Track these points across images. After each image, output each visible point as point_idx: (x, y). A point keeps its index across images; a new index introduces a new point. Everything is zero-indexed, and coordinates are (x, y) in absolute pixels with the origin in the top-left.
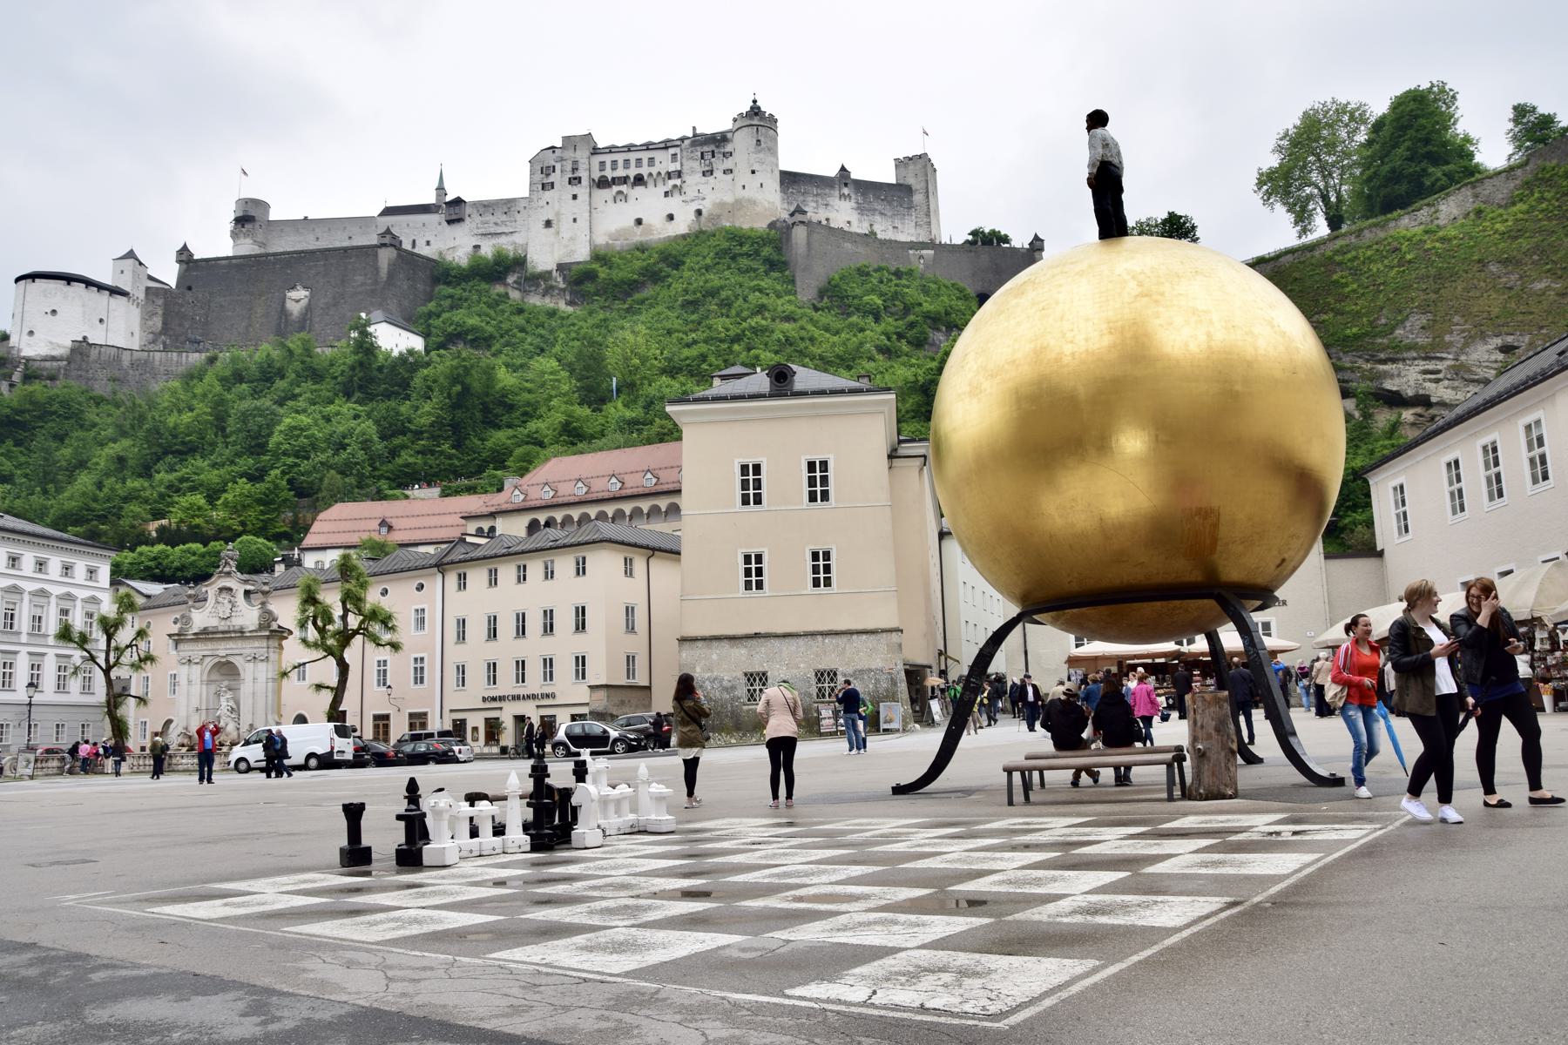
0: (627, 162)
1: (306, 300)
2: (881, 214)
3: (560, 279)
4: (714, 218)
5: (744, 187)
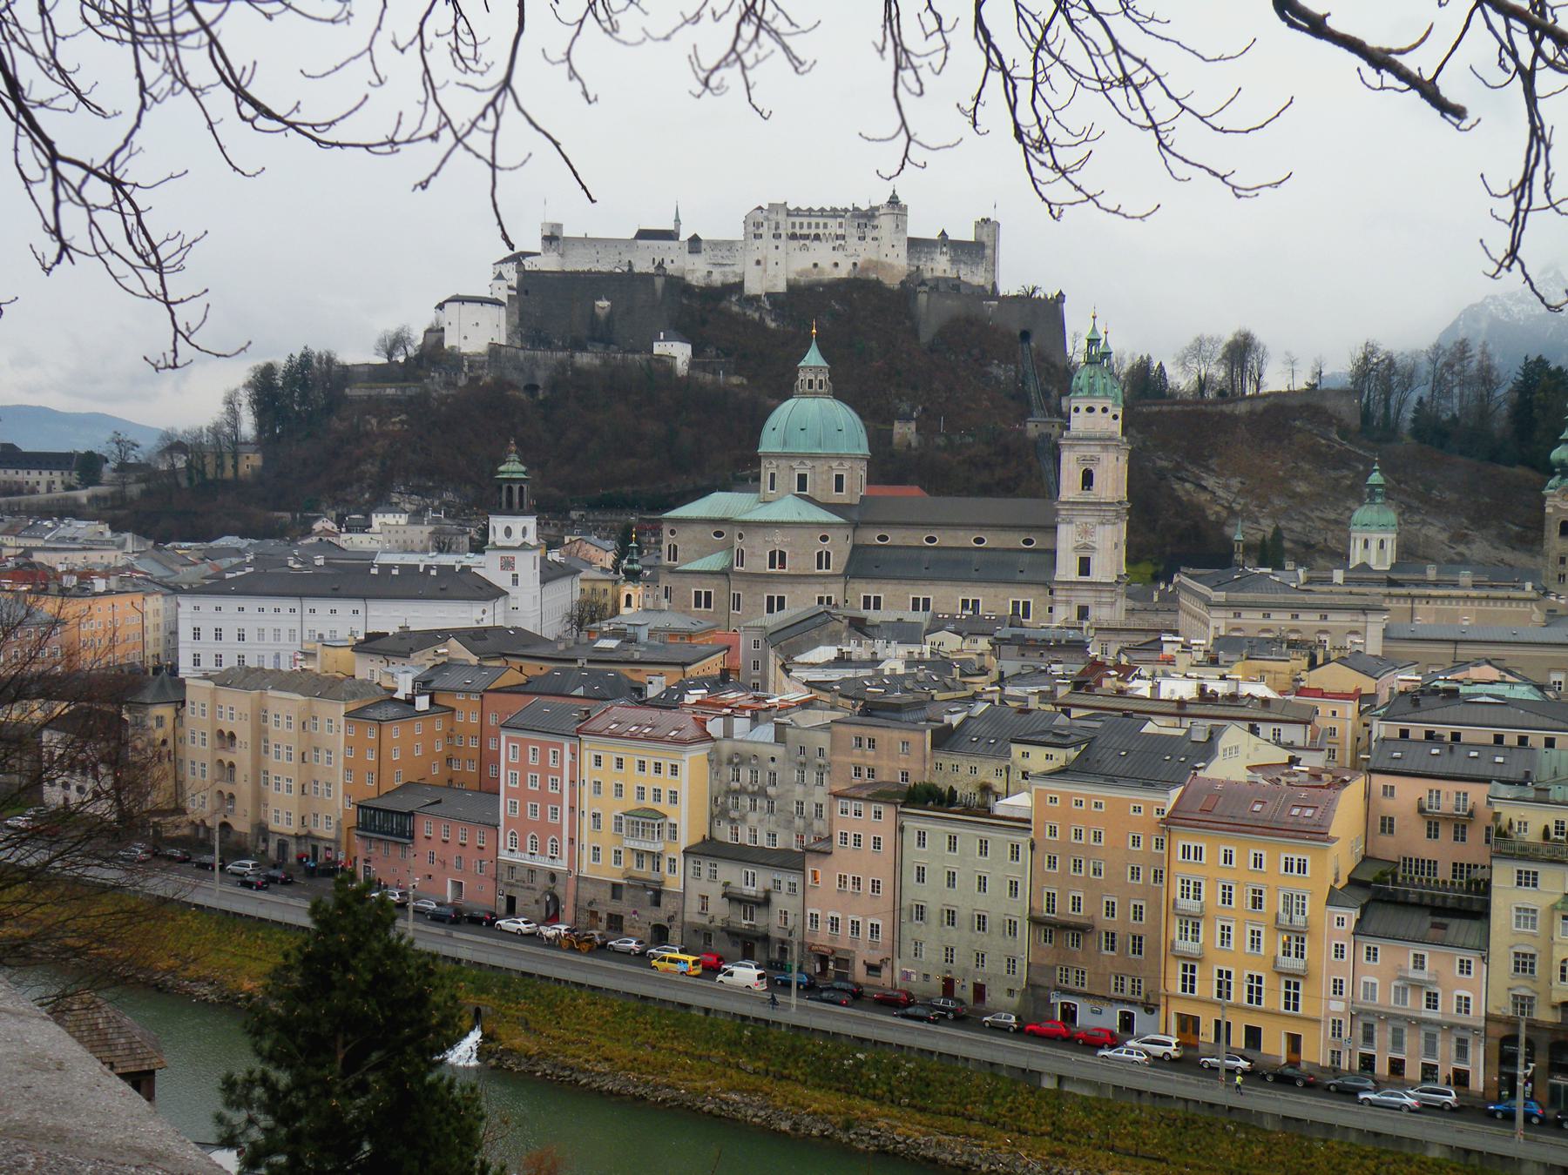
0: (809, 225)
3: (767, 303)
4: (865, 269)
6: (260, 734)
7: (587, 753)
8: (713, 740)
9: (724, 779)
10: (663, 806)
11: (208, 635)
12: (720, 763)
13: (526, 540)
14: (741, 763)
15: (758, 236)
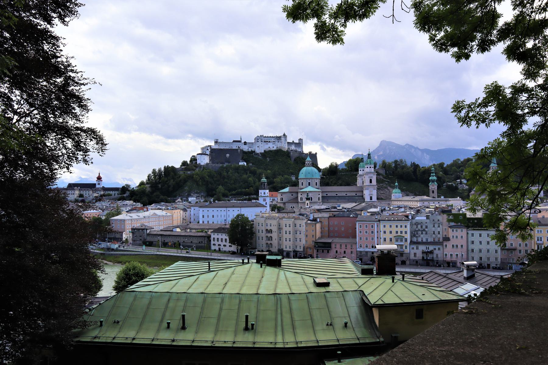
6: (280, 229)
7: (381, 225)
9: (414, 228)
10: (403, 234)
11: (206, 217)
12: (413, 225)
14: (418, 224)
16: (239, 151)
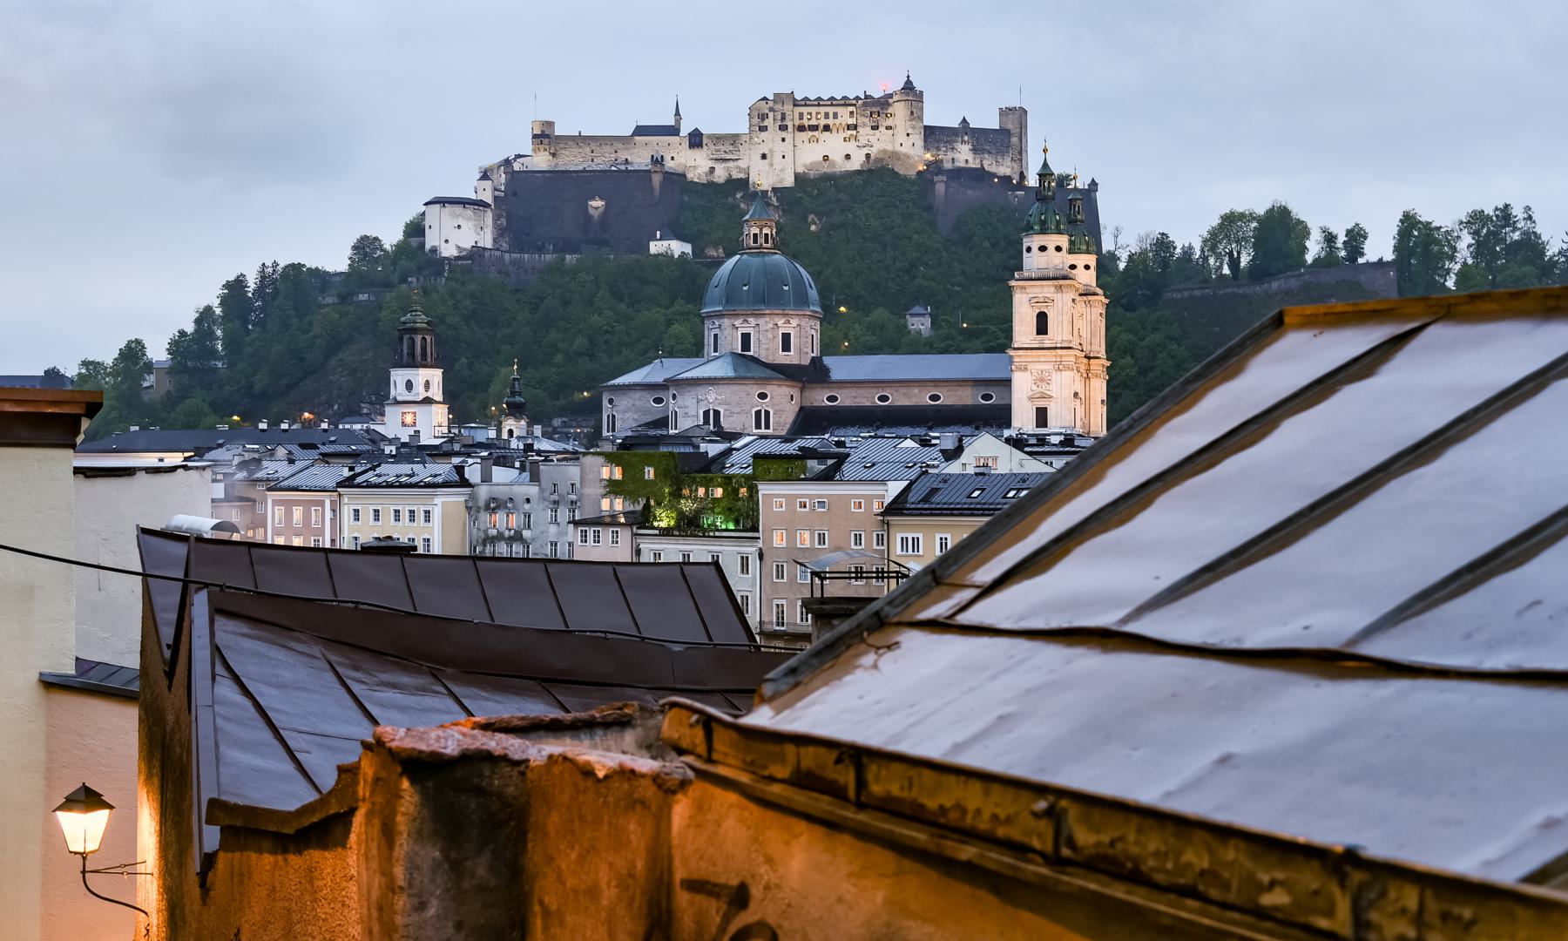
1: (603, 208)
2: (989, 153)
3: (774, 199)
4: (878, 160)
5: (901, 145)
7: (346, 507)
8: (470, 485)
13: (429, 394)
15: (763, 129)
16: (657, 179)
